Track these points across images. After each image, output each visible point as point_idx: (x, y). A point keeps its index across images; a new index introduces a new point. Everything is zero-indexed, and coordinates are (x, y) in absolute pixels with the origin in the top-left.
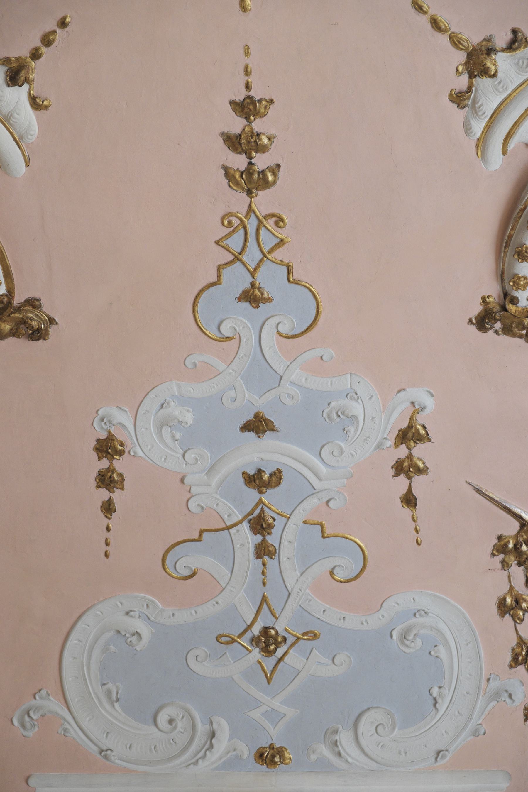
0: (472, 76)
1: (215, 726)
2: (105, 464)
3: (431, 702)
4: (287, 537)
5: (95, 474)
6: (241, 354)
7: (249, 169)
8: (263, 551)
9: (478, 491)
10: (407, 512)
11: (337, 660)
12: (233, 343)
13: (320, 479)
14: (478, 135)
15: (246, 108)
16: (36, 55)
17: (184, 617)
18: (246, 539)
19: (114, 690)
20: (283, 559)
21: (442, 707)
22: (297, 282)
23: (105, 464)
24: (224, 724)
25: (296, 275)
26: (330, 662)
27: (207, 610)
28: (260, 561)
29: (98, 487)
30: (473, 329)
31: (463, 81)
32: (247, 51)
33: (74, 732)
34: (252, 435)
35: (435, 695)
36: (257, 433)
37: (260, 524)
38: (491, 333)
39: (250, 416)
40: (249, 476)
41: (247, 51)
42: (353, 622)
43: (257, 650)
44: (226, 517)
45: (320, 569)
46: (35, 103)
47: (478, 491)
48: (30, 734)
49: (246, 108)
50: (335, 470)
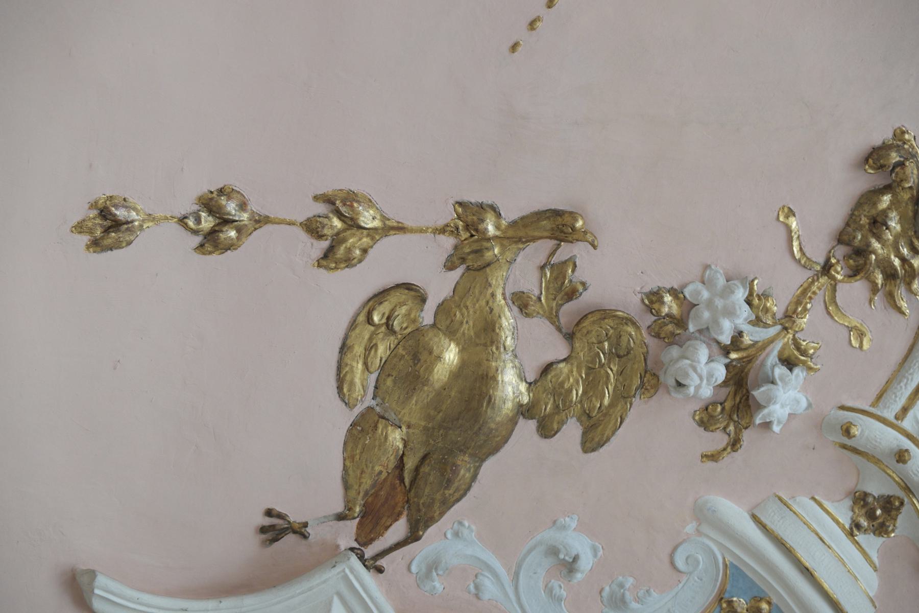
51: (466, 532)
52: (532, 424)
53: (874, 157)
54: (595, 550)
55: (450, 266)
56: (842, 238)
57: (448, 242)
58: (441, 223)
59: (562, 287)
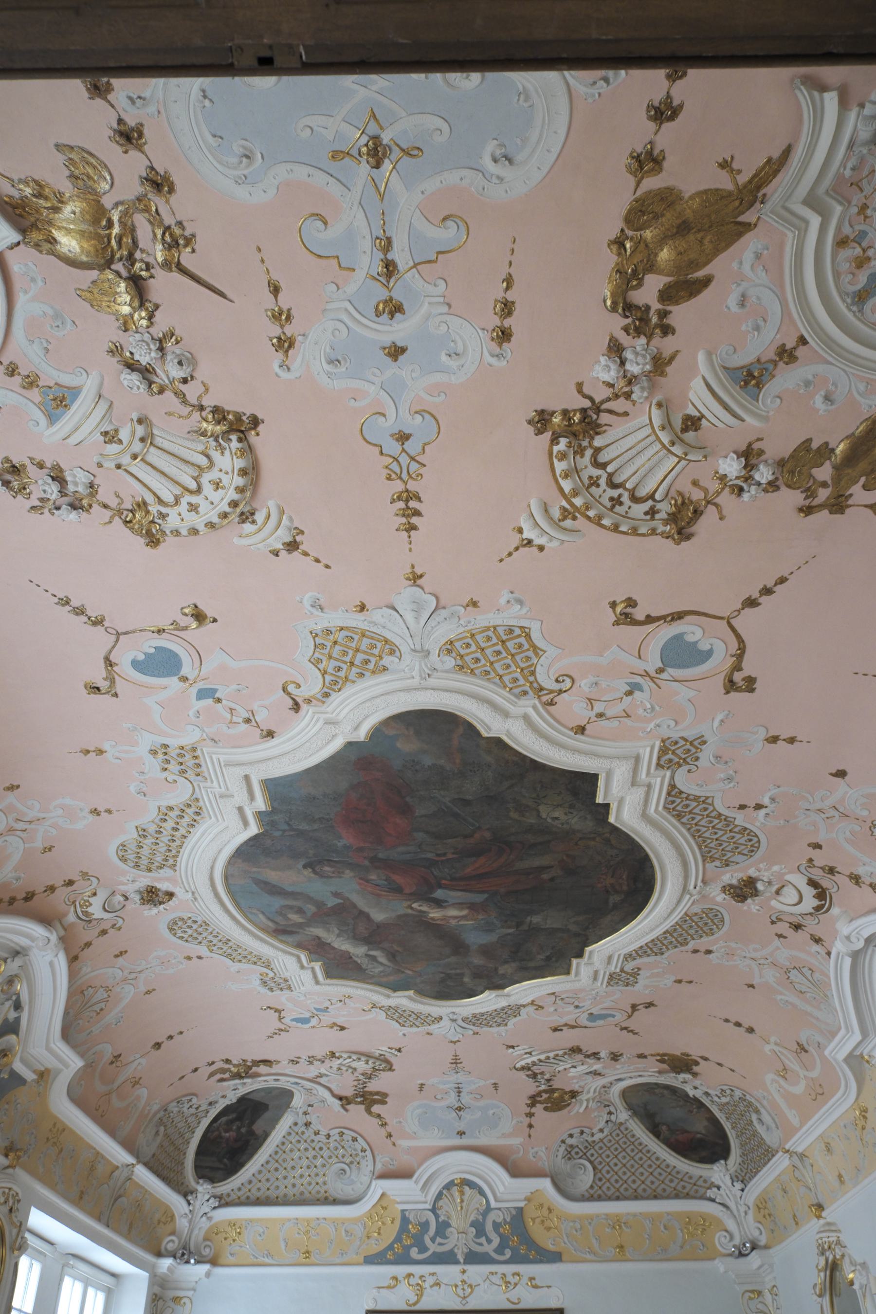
0: (295, 541)
3: (208, 93)
4: (368, 261)
5: (515, 314)
7: (407, 501)
8: (387, 245)
10: (275, 276)
11: (309, 131)
12: (414, 409)
13: (346, 310)
14: (284, 517)
16: (517, 549)
17: (451, 178)
18: (400, 256)
20: (368, 237)
22: (375, 445)
23: (507, 323)
25: (377, 449)
26: (315, 128)
27: (432, 185)
28: (388, 235)
29: (513, 303)
30: (260, 416)
31: (298, 539)
32: (410, 550)
34: (400, 344)
36: (395, 346)
37: (390, 268)
38: (248, 415)
39: (401, 358)
40: (400, 312)
41: (410, 550)
42: (301, 172)
43: (385, 142)
44: (417, 276)
45: (335, 230)
46: (520, 531)
50: (335, 315)
52: (830, 446)
53: (689, 537)
54: (814, 403)
55: (851, 495)
56: (702, 513)
57: (850, 502)
59: (810, 493)
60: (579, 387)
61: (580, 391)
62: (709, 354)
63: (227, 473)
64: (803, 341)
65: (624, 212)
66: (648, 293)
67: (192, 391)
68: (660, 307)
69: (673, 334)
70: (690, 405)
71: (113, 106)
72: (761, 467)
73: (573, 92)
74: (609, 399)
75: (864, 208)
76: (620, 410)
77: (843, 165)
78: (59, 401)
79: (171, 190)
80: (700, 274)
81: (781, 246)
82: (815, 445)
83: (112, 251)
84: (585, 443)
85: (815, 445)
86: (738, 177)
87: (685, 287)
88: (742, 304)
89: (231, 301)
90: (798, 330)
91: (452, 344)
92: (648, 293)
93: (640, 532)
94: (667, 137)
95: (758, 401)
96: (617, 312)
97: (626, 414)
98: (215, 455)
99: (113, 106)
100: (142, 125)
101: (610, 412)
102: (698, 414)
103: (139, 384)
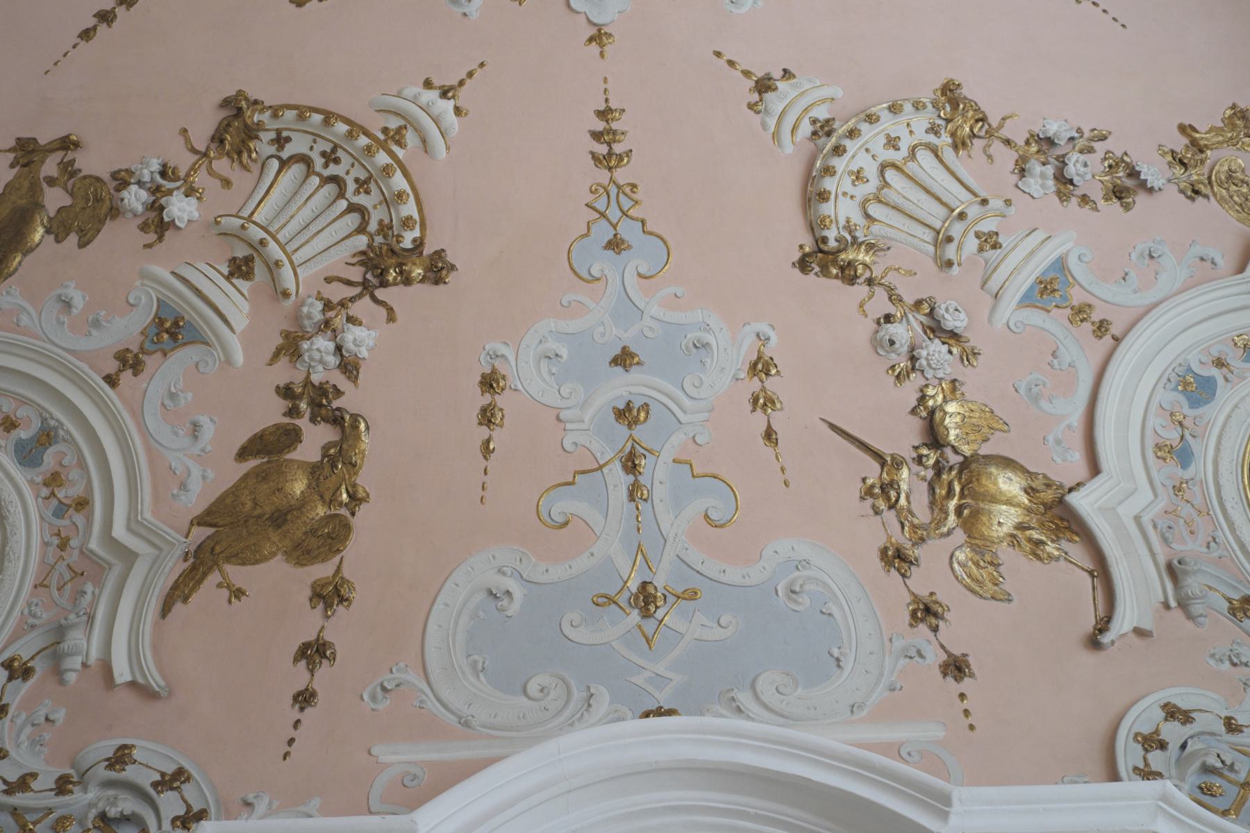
0: (760, 93)
1: (592, 691)
2: (487, 399)
3: (833, 663)
4: (657, 472)
5: (477, 411)
6: (607, 294)
7: (610, 154)
8: (634, 493)
9: (833, 427)
10: (769, 451)
11: (723, 622)
12: (601, 284)
13: (685, 412)
14: (772, 129)
15: (604, 114)
16: (461, 83)
17: (558, 572)
18: (618, 479)
19: (481, 661)
20: (656, 501)
21: (848, 665)
22: (650, 233)
23: (487, 399)
24: (602, 688)
25: (649, 228)
26: (715, 625)
27: (582, 563)
28: (633, 504)
29: (480, 424)
30: (797, 271)
31: (756, 97)
32: (605, 80)
33: (433, 705)
34: (619, 369)
35: (836, 655)
36: (625, 367)
37: (631, 464)
39: (618, 351)
40: (619, 410)
41: (605, 80)
42: (733, 575)
43: (636, 611)
44: (598, 455)
45: (694, 510)
46: (458, 111)
47: (833, 427)
48: (380, 707)
49: (604, 114)
51: (12, 291)
52: (52, 237)
53: (226, 103)
54: (84, 297)
55: (12, 166)
56: (213, 139)
57: (11, 156)
58: (8, 147)
59: (68, 169)
60: (391, 317)
61: (390, 310)
62: (229, 361)
63: (845, 194)
64: (111, 381)
65: (353, 537)
66: (315, 439)
67: (881, 304)
68: (297, 422)
69: (278, 387)
70: (246, 293)
71: (942, 647)
72: (140, 209)
73: (422, 674)
74: (352, 300)
75: (63, 546)
76: (335, 284)
77: (96, 599)
78: (1047, 289)
79: (884, 551)
80: (253, 463)
81: (156, 497)
82: (73, 238)
83: (960, 479)
84: (379, 240)
85: (73, 238)
86: (220, 579)
87: (270, 446)
88: (196, 427)
89: (823, 420)
90: (120, 395)
91: (554, 370)
92: (315, 439)
93: (295, 112)
94: (309, 624)
95: (158, 300)
96: (351, 415)
97: (329, 280)
98: (857, 219)
99: (942, 647)
100: (911, 625)
101: (349, 283)
102: (234, 281)
103: (947, 316)
